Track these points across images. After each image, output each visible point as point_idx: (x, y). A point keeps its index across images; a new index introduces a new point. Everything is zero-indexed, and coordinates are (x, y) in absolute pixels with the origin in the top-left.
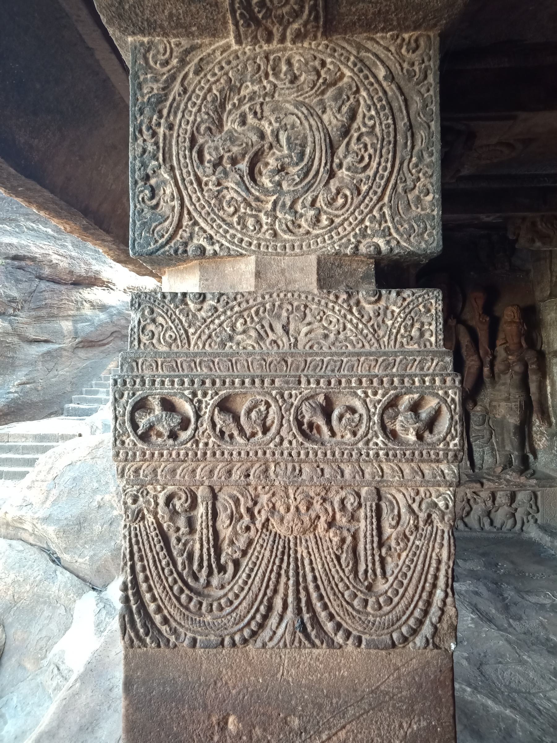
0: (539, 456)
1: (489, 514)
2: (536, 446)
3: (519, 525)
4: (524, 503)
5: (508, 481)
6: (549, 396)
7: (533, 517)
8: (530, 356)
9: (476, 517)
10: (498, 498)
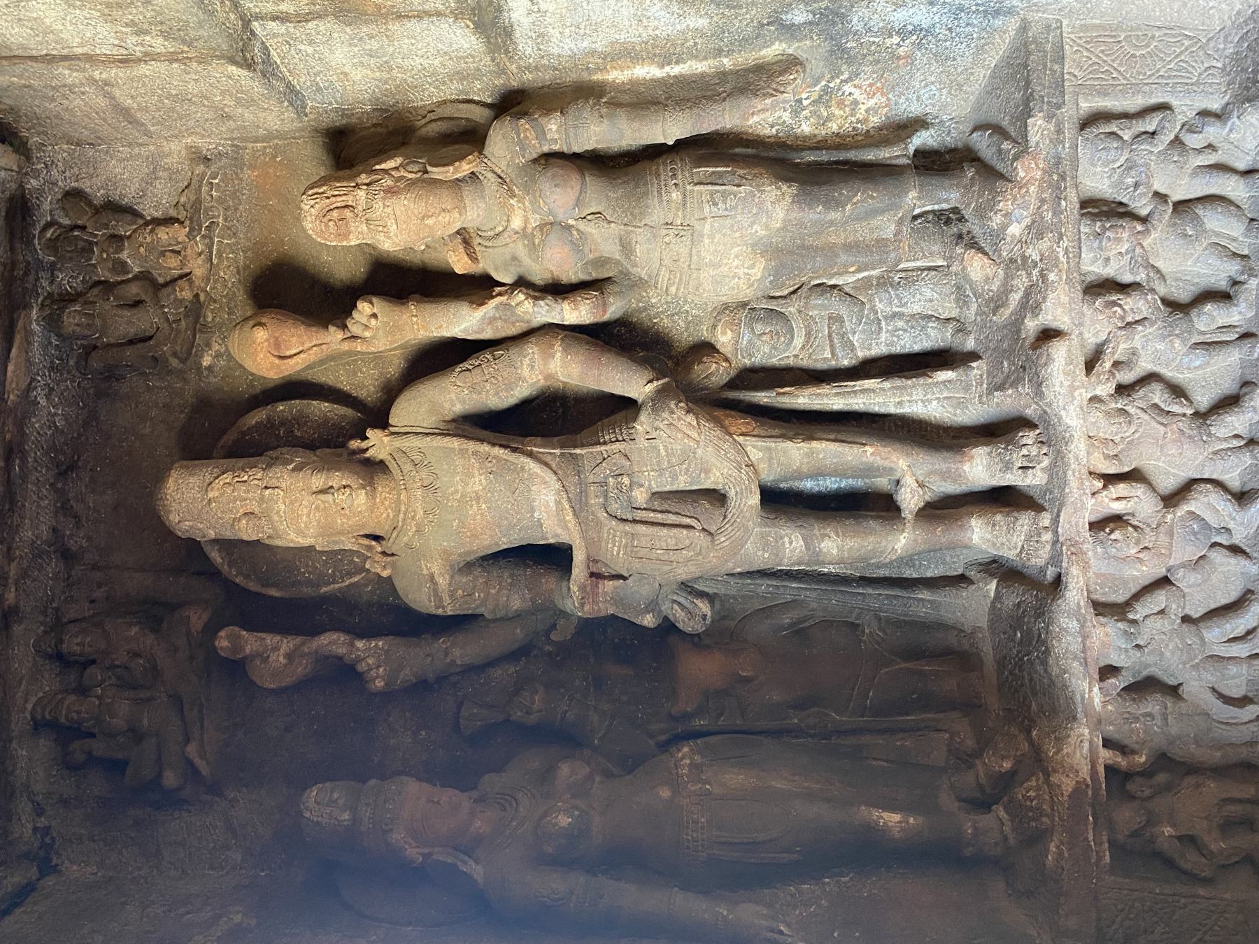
0: (915, 110)
1: (1177, 307)
2: (875, 120)
3: (1233, 187)
4: (1129, 167)
5: (1037, 230)
6: (676, 70)
7: (1190, 128)
8: (506, 146)
9: (1199, 358)
10: (1109, 271)
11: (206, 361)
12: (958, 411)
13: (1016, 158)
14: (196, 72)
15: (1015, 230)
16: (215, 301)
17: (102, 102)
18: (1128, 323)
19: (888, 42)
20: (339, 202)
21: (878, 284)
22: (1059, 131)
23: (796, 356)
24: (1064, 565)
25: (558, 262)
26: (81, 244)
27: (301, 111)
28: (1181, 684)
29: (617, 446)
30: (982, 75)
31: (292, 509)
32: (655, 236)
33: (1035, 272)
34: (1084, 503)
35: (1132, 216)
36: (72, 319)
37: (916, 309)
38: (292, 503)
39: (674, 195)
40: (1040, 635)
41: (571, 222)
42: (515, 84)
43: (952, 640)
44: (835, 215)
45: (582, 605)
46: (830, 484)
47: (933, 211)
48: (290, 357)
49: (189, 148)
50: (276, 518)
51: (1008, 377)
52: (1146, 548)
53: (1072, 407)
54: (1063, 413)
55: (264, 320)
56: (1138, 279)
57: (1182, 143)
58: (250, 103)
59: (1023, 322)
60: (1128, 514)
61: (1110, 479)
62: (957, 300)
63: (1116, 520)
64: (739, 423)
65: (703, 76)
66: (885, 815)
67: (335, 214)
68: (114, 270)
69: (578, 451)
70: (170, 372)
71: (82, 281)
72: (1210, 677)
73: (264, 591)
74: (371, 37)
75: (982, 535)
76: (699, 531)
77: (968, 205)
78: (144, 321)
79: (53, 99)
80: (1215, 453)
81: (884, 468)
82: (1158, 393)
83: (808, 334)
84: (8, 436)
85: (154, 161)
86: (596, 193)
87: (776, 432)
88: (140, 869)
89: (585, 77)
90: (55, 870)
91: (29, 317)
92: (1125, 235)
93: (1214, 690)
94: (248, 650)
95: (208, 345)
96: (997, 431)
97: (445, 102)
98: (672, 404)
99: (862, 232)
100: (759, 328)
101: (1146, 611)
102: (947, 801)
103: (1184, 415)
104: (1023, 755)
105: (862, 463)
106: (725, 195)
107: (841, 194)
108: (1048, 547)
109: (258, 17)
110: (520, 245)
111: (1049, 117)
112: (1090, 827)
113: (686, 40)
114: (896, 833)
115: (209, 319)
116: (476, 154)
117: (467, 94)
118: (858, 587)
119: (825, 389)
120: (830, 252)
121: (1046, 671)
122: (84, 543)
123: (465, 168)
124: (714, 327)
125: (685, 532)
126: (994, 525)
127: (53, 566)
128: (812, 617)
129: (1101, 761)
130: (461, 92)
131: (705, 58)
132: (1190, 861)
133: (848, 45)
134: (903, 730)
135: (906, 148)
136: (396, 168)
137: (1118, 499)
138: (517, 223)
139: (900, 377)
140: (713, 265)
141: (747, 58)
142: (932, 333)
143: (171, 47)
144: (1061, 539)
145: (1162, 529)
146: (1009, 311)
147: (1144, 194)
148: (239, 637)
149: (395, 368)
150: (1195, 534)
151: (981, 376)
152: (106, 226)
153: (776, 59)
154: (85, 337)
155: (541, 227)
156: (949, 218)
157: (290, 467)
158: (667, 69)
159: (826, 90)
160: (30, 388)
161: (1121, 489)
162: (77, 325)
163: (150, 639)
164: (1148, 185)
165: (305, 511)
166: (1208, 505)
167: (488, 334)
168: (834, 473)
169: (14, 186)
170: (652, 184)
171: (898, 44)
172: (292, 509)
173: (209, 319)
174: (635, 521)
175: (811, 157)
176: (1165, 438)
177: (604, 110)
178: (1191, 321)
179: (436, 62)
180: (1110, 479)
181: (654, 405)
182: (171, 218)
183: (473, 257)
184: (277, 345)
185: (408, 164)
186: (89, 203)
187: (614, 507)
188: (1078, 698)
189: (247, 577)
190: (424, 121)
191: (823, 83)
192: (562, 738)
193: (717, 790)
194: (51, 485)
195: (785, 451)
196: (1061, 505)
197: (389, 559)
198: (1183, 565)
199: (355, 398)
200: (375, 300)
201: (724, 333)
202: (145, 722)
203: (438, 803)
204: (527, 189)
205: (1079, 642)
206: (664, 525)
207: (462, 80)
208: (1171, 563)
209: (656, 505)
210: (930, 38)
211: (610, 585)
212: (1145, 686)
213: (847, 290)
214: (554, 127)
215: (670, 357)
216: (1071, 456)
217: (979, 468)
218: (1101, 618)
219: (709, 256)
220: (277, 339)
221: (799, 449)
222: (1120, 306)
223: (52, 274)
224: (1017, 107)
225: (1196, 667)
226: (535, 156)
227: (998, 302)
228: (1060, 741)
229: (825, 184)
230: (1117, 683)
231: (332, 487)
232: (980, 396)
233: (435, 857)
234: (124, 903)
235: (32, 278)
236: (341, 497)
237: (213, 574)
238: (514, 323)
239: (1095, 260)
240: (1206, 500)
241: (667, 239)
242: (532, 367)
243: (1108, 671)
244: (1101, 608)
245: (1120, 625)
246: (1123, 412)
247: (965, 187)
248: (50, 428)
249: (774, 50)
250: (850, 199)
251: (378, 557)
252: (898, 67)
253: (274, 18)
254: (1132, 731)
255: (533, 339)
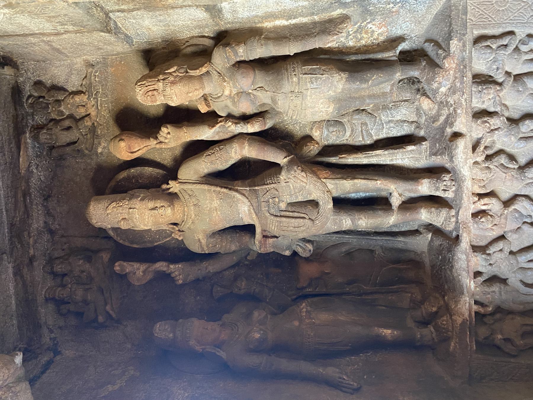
0: (399, 32)
1: (513, 121)
2: (382, 38)
4: (495, 61)
5: (453, 90)
6: (293, 21)
8: (221, 59)
9: (522, 144)
10: (484, 107)
11: (100, 150)
12: (417, 163)
13: (444, 58)
14: (87, 36)
15: (443, 90)
16: (101, 125)
17: (47, 48)
18: (492, 130)
19: (388, 6)
20: (151, 88)
21: (382, 108)
22: (464, 46)
23: (347, 140)
24: (461, 232)
25: (245, 107)
26: (44, 105)
27: (131, 44)
28: (507, 279)
29: (272, 186)
30: (430, 17)
31: (141, 216)
32: (286, 97)
33: (451, 109)
34: (469, 205)
35: (496, 83)
36: (44, 136)
37: (399, 118)
38: (141, 214)
39: (294, 79)
40: (449, 259)
41: (250, 91)
42: (223, 29)
43: (412, 256)
44: (364, 86)
45: (260, 248)
46: (362, 195)
47: (407, 78)
48: (135, 152)
49: (84, 60)
50: (135, 220)
51: (438, 150)
52: (495, 224)
53: (466, 167)
54: (462, 170)
55: (123, 138)
56: (497, 110)
57: (519, 50)
58: (110, 44)
59: (445, 129)
60: (488, 210)
61: (481, 196)
62: (417, 115)
63: (483, 213)
64: (324, 173)
65: (305, 24)
66: (385, 331)
67: (150, 93)
68: (58, 115)
69: (256, 188)
70: (85, 155)
71: (45, 119)
72: (520, 276)
73: (131, 246)
74: (160, 15)
75: (425, 215)
76: (308, 219)
77: (423, 78)
78: (73, 135)
79: (27, 48)
80: (526, 184)
81: (385, 189)
82: (503, 159)
83: (352, 131)
84: (23, 188)
85: (70, 67)
86: (260, 78)
87: (339, 176)
88: (92, 351)
89: (254, 25)
90: (59, 353)
91: (26, 137)
92: (492, 91)
93: (521, 281)
94: (127, 271)
95: (100, 144)
96: (434, 172)
97: (193, 37)
98: (295, 168)
99: (376, 90)
100: (331, 129)
101: (494, 250)
102: (410, 323)
103: (514, 169)
104: (441, 306)
105: (376, 188)
106: (316, 79)
107: (367, 76)
108: (454, 224)
109: (111, 11)
110: (228, 101)
111: (460, 40)
112: (468, 336)
113: (298, 10)
114: (389, 338)
115: (99, 133)
116: (208, 63)
117: (202, 33)
118: (373, 236)
119: (360, 155)
120: (362, 99)
121: (451, 274)
122: (57, 227)
123: (204, 70)
124: (312, 129)
125: (302, 220)
126: (431, 213)
127: (46, 237)
128: (354, 248)
129: (473, 310)
130: (200, 33)
131: (307, 16)
132: (508, 348)
133: (370, 9)
134: (392, 292)
135: (395, 52)
136: (174, 72)
137: (484, 205)
138: (227, 93)
139: (392, 149)
140: (312, 108)
141: (325, 16)
142: (406, 128)
143: (75, 28)
144: (460, 221)
145: (502, 217)
146: (439, 123)
147: (501, 73)
148: (123, 265)
149: (178, 152)
150: (516, 218)
151: (427, 148)
152: (53, 96)
153: (338, 16)
154: (49, 143)
155: (237, 94)
156: (414, 81)
157: (139, 199)
158: (290, 21)
159: (360, 27)
160: (29, 166)
161: (486, 200)
162: (45, 139)
163: (88, 266)
164: (503, 69)
165: (147, 217)
166: (522, 206)
167: (216, 138)
168: (364, 191)
169: (13, 82)
170: (285, 74)
171: (393, 7)
172: (141, 216)
173: (99, 133)
174: (281, 216)
175: (354, 58)
176: (505, 178)
177: (263, 42)
178: (519, 128)
179: (189, 23)
180: (481, 196)
181: (288, 168)
182: (80, 91)
183: (208, 105)
184: (130, 148)
185: (179, 69)
186: (45, 87)
187: (272, 211)
188: (465, 285)
189: (124, 240)
190: (184, 46)
191: (359, 24)
192: (253, 299)
193: (317, 322)
194: (42, 204)
195: (343, 184)
196: (460, 208)
197: (182, 233)
198: (511, 231)
199: (162, 164)
200: (168, 126)
201: (316, 132)
202: (89, 298)
203: (207, 329)
204: (230, 78)
205: (466, 263)
206: (293, 217)
207: (201, 28)
208: (506, 230)
209: (290, 209)
210: (407, 4)
211: (271, 240)
212: (494, 279)
213: (369, 111)
214: (241, 51)
215: (293, 142)
216: (465, 187)
217: (425, 187)
218: (475, 253)
219: (311, 103)
220: (129, 145)
221: (349, 183)
222: (488, 123)
223: (33, 117)
224: (445, 34)
225: (514, 272)
226: (233, 63)
227: (435, 119)
228: (457, 302)
229: (360, 72)
230: (481, 279)
231: (157, 207)
232: (426, 157)
233: (207, 350)
234: (88, 367)
235: (25, 121)
236: (161, 211)
237: (109, 238)
238: (227, 133)
239: (478, 102)
240: (522, 204)
241: (291, 98)
242: (236, 153)
243: (478, 274)
244: (476, 249)
245: (483, 256)
246: (488, 168)
247: (421, 70)
248: (39, 181)
249: (337, 12)
250: (371, 78)
251: (177, 232)
252: (392, 16)
253: (118, 11)
254: (487, 298)
255: (236, 141)
